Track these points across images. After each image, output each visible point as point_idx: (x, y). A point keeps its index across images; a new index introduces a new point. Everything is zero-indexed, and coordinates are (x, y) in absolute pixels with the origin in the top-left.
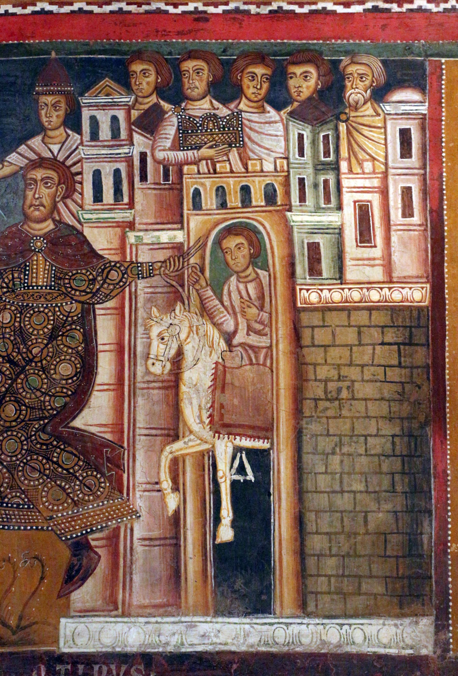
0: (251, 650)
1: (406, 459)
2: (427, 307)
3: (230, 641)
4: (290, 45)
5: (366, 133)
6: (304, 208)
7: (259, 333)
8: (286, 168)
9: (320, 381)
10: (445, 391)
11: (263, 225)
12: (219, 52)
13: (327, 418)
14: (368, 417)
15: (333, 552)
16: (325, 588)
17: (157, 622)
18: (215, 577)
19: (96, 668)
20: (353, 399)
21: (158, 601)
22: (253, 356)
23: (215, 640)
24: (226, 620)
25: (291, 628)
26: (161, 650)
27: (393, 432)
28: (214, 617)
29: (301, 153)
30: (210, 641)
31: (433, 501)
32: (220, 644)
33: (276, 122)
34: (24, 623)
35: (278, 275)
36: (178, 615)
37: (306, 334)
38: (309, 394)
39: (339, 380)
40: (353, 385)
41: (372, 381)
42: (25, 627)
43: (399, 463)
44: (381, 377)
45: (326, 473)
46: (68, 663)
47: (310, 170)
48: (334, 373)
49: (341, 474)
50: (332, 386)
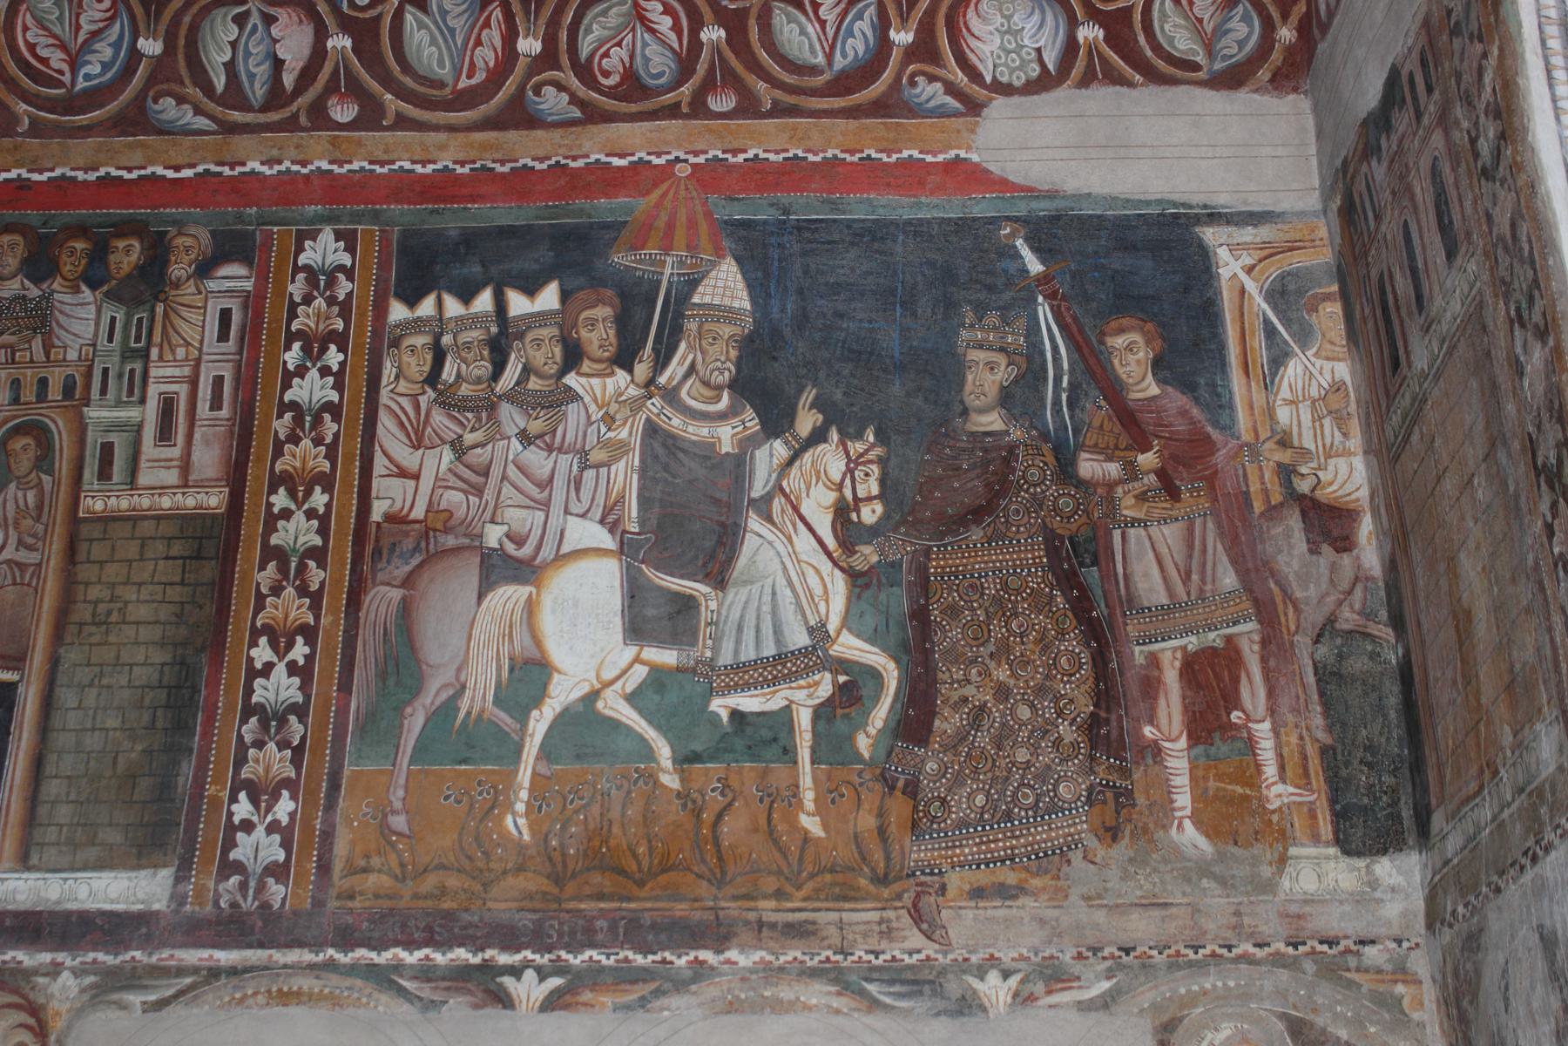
1: (173, 690)
2: (223, 514)
4: (115, 214)
5: (185, 314)
6: (104, 403)
7: (30, 548)
8: (91, 356)
9: (90, 602)
10: (229, 612)
11: (55, 422)
12: (39, 224)
13: (91, 645)
14: (137, 643)
15: (71, 798)
16: (53, 838)
20: (124, 623)
22: (18, 574)
27: (163, 660)
29: (110, 340)
31: (197, 738)
33: (89, 304)
35: (63, 481)
37: (84, 546)
38: (75, 618)
39: (111, 601)
40: (126, 607)
41: (147, 601)
43: (164, 696)
44: (159, 597)
45: (79, 708)
47: (117, 359)
48: (106, 594)
49: (97, 708)
50: (102, 608)
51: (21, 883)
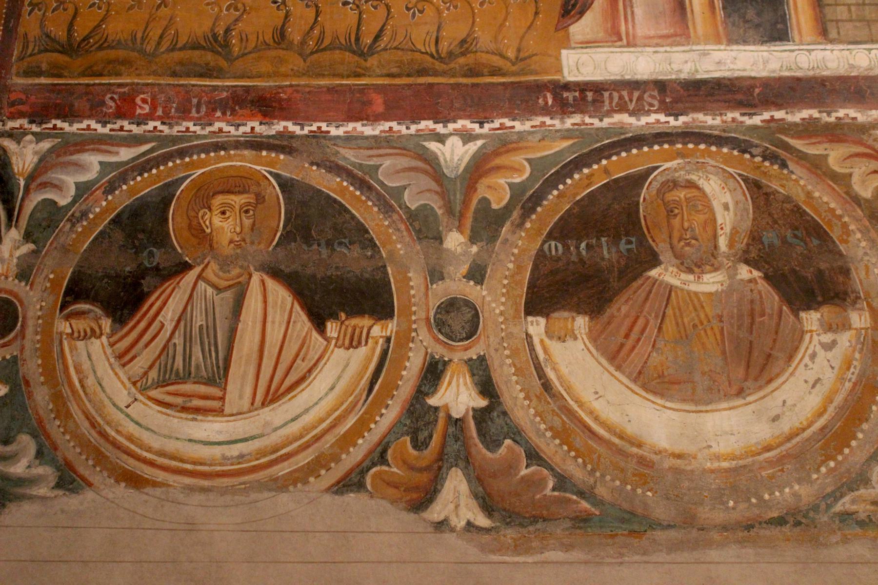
0: (773, 75)
3: (748, 67)
17: (666, 52)
18: (724, 8)
19: (606, 94)
21: (665, 32)
23: (732, 66)
24: (742, 47)
25: (813, 53)
26: (674, 77)
28: (728, 45)
30: (727, 68)
32: (738, 70)
34: (522, 55)
36: (689, 44)
42: (522, 60)
46: (575, 91)
51: (828, 53)
